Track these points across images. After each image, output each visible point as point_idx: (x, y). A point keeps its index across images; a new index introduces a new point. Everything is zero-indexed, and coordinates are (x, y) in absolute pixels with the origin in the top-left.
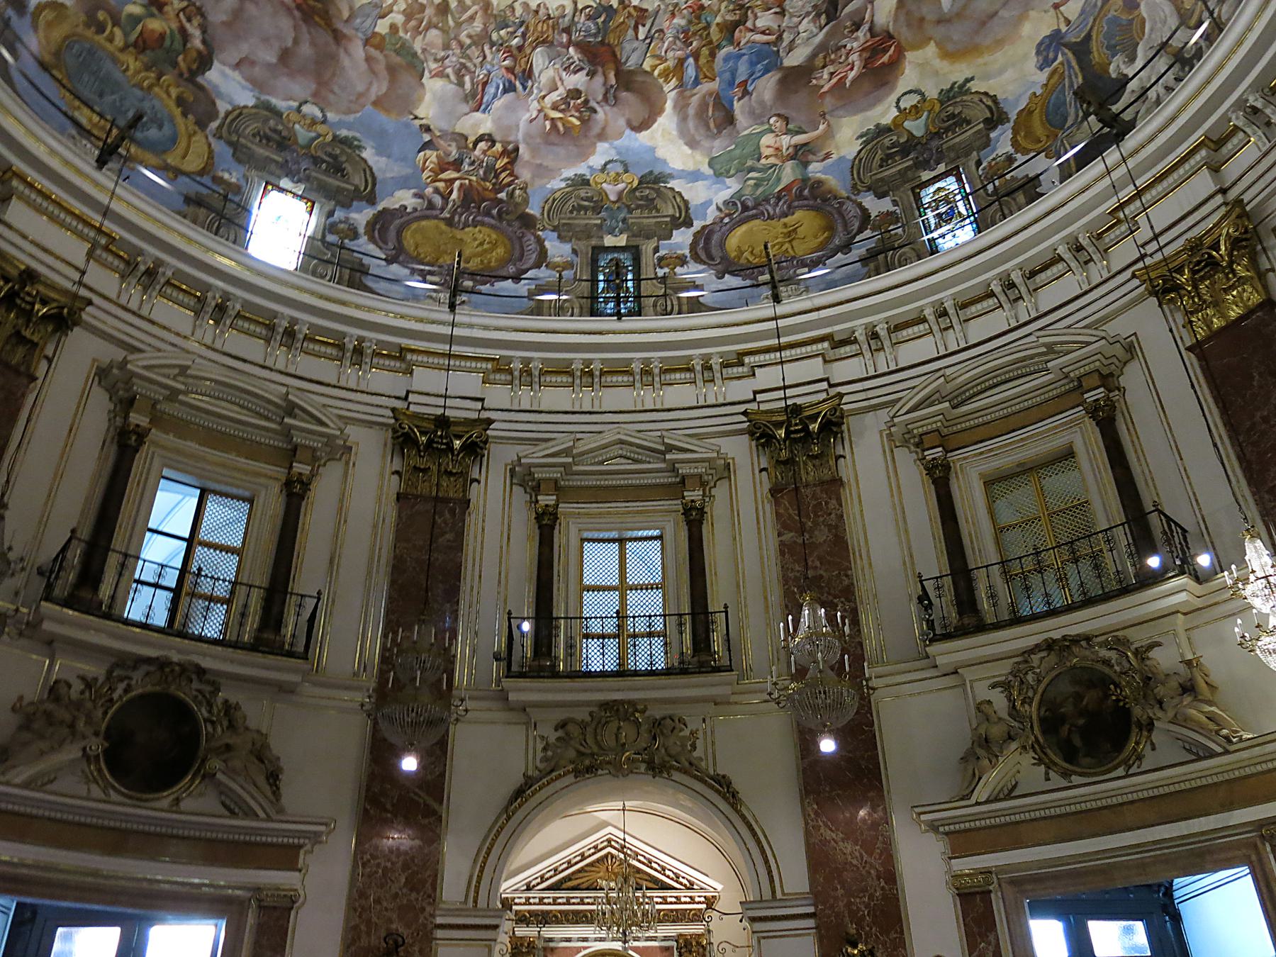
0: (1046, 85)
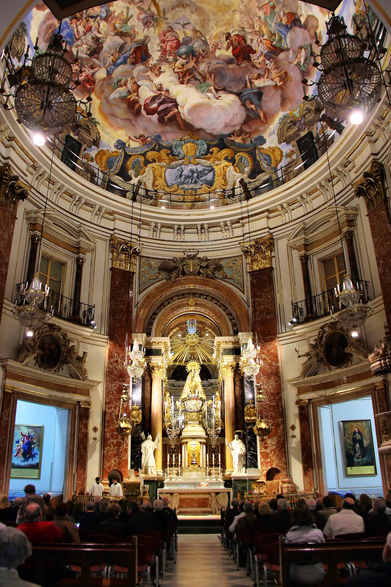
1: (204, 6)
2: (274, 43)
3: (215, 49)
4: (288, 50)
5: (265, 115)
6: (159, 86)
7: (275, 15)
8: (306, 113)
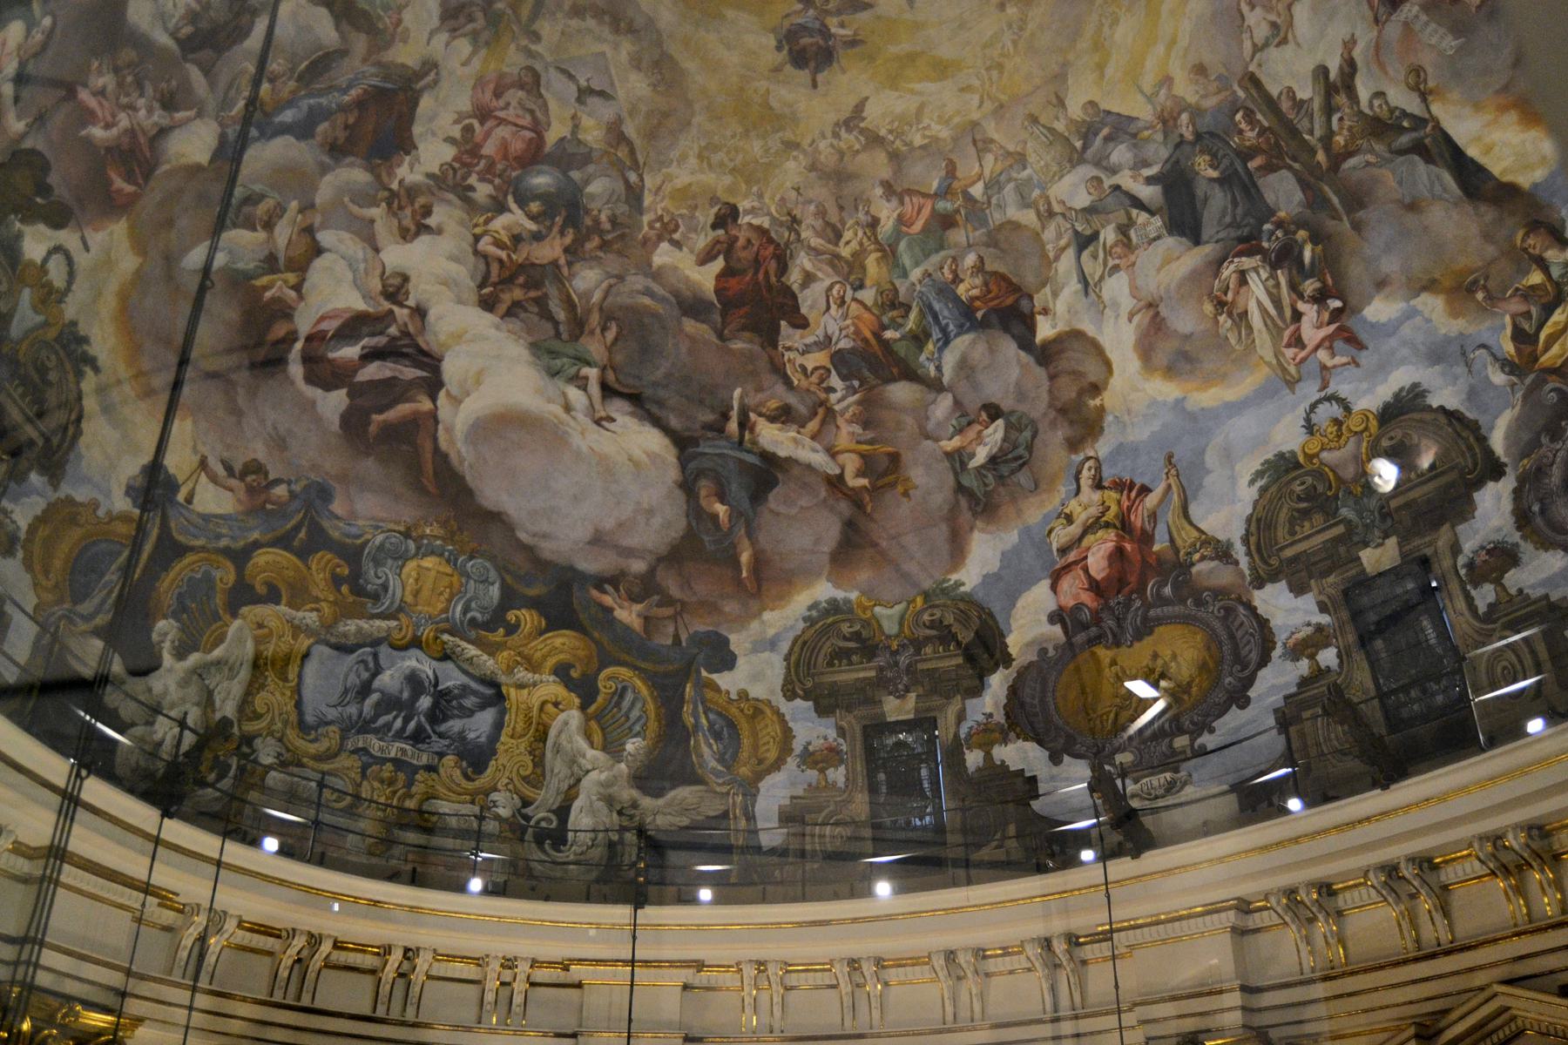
0: (112, 518)
1: (690, 65)
2: (889, 334)
3: (660, 238)
4: (936, 386)
5: (760, 563)
6: (397, 281)
7: (942, 247)
8: (928, 639)
